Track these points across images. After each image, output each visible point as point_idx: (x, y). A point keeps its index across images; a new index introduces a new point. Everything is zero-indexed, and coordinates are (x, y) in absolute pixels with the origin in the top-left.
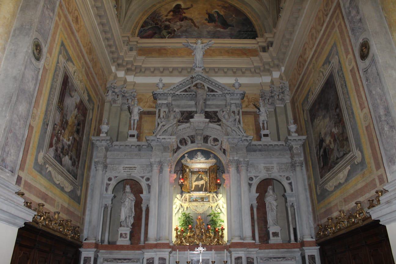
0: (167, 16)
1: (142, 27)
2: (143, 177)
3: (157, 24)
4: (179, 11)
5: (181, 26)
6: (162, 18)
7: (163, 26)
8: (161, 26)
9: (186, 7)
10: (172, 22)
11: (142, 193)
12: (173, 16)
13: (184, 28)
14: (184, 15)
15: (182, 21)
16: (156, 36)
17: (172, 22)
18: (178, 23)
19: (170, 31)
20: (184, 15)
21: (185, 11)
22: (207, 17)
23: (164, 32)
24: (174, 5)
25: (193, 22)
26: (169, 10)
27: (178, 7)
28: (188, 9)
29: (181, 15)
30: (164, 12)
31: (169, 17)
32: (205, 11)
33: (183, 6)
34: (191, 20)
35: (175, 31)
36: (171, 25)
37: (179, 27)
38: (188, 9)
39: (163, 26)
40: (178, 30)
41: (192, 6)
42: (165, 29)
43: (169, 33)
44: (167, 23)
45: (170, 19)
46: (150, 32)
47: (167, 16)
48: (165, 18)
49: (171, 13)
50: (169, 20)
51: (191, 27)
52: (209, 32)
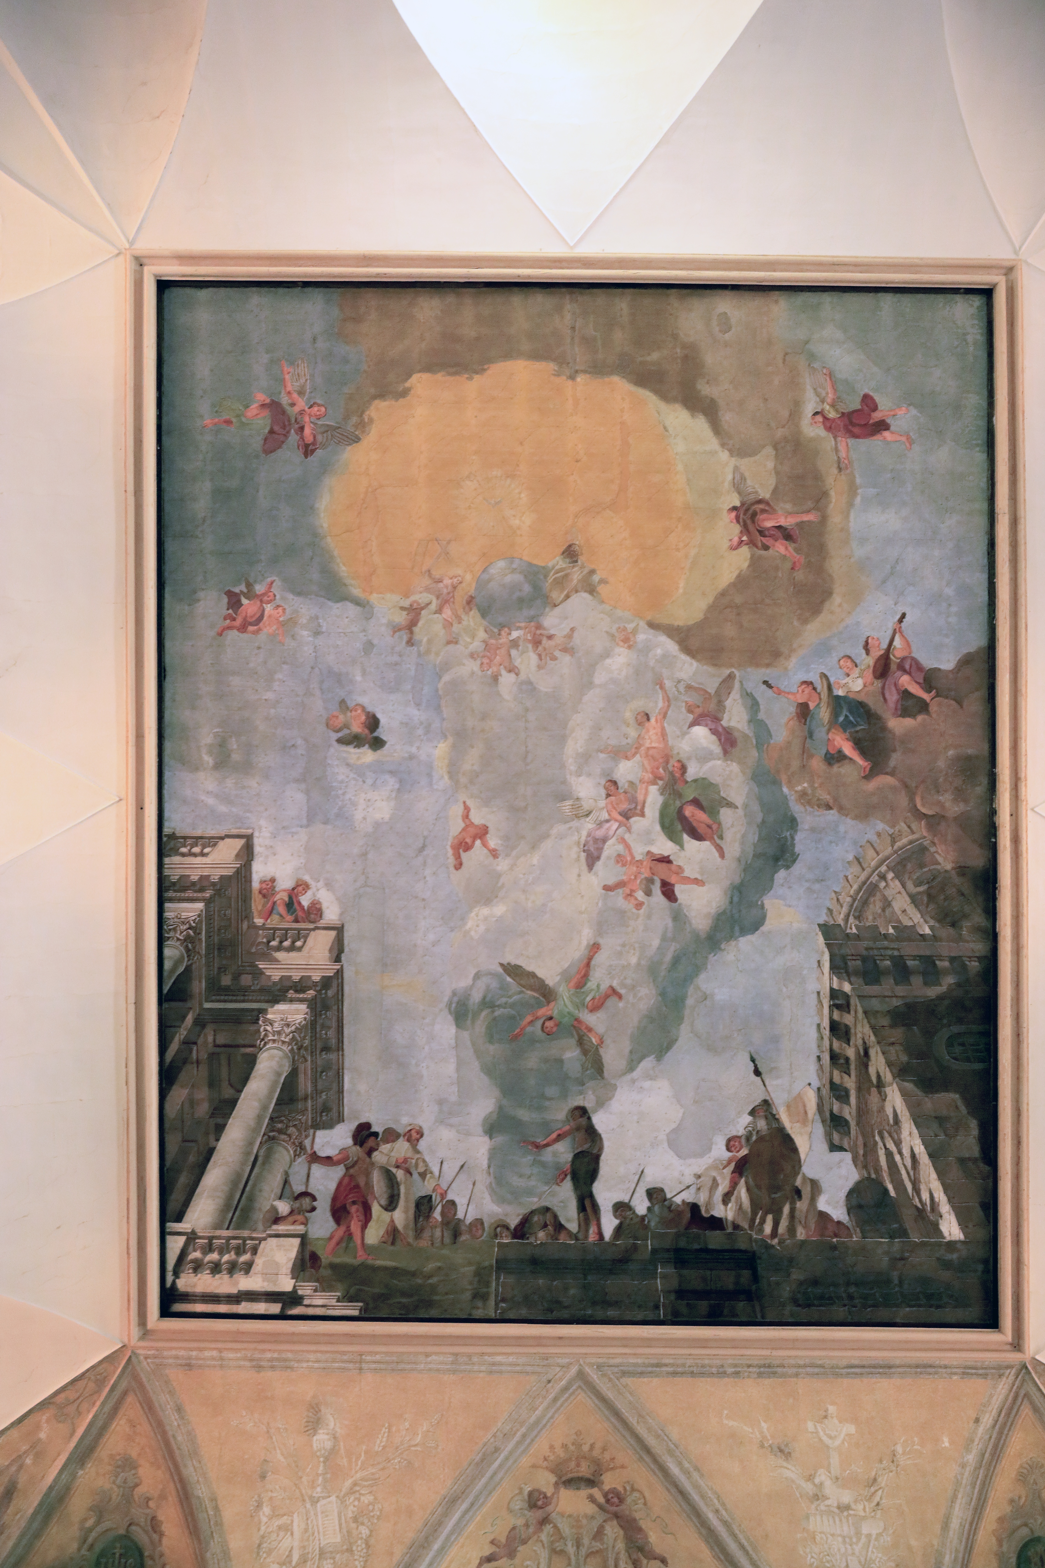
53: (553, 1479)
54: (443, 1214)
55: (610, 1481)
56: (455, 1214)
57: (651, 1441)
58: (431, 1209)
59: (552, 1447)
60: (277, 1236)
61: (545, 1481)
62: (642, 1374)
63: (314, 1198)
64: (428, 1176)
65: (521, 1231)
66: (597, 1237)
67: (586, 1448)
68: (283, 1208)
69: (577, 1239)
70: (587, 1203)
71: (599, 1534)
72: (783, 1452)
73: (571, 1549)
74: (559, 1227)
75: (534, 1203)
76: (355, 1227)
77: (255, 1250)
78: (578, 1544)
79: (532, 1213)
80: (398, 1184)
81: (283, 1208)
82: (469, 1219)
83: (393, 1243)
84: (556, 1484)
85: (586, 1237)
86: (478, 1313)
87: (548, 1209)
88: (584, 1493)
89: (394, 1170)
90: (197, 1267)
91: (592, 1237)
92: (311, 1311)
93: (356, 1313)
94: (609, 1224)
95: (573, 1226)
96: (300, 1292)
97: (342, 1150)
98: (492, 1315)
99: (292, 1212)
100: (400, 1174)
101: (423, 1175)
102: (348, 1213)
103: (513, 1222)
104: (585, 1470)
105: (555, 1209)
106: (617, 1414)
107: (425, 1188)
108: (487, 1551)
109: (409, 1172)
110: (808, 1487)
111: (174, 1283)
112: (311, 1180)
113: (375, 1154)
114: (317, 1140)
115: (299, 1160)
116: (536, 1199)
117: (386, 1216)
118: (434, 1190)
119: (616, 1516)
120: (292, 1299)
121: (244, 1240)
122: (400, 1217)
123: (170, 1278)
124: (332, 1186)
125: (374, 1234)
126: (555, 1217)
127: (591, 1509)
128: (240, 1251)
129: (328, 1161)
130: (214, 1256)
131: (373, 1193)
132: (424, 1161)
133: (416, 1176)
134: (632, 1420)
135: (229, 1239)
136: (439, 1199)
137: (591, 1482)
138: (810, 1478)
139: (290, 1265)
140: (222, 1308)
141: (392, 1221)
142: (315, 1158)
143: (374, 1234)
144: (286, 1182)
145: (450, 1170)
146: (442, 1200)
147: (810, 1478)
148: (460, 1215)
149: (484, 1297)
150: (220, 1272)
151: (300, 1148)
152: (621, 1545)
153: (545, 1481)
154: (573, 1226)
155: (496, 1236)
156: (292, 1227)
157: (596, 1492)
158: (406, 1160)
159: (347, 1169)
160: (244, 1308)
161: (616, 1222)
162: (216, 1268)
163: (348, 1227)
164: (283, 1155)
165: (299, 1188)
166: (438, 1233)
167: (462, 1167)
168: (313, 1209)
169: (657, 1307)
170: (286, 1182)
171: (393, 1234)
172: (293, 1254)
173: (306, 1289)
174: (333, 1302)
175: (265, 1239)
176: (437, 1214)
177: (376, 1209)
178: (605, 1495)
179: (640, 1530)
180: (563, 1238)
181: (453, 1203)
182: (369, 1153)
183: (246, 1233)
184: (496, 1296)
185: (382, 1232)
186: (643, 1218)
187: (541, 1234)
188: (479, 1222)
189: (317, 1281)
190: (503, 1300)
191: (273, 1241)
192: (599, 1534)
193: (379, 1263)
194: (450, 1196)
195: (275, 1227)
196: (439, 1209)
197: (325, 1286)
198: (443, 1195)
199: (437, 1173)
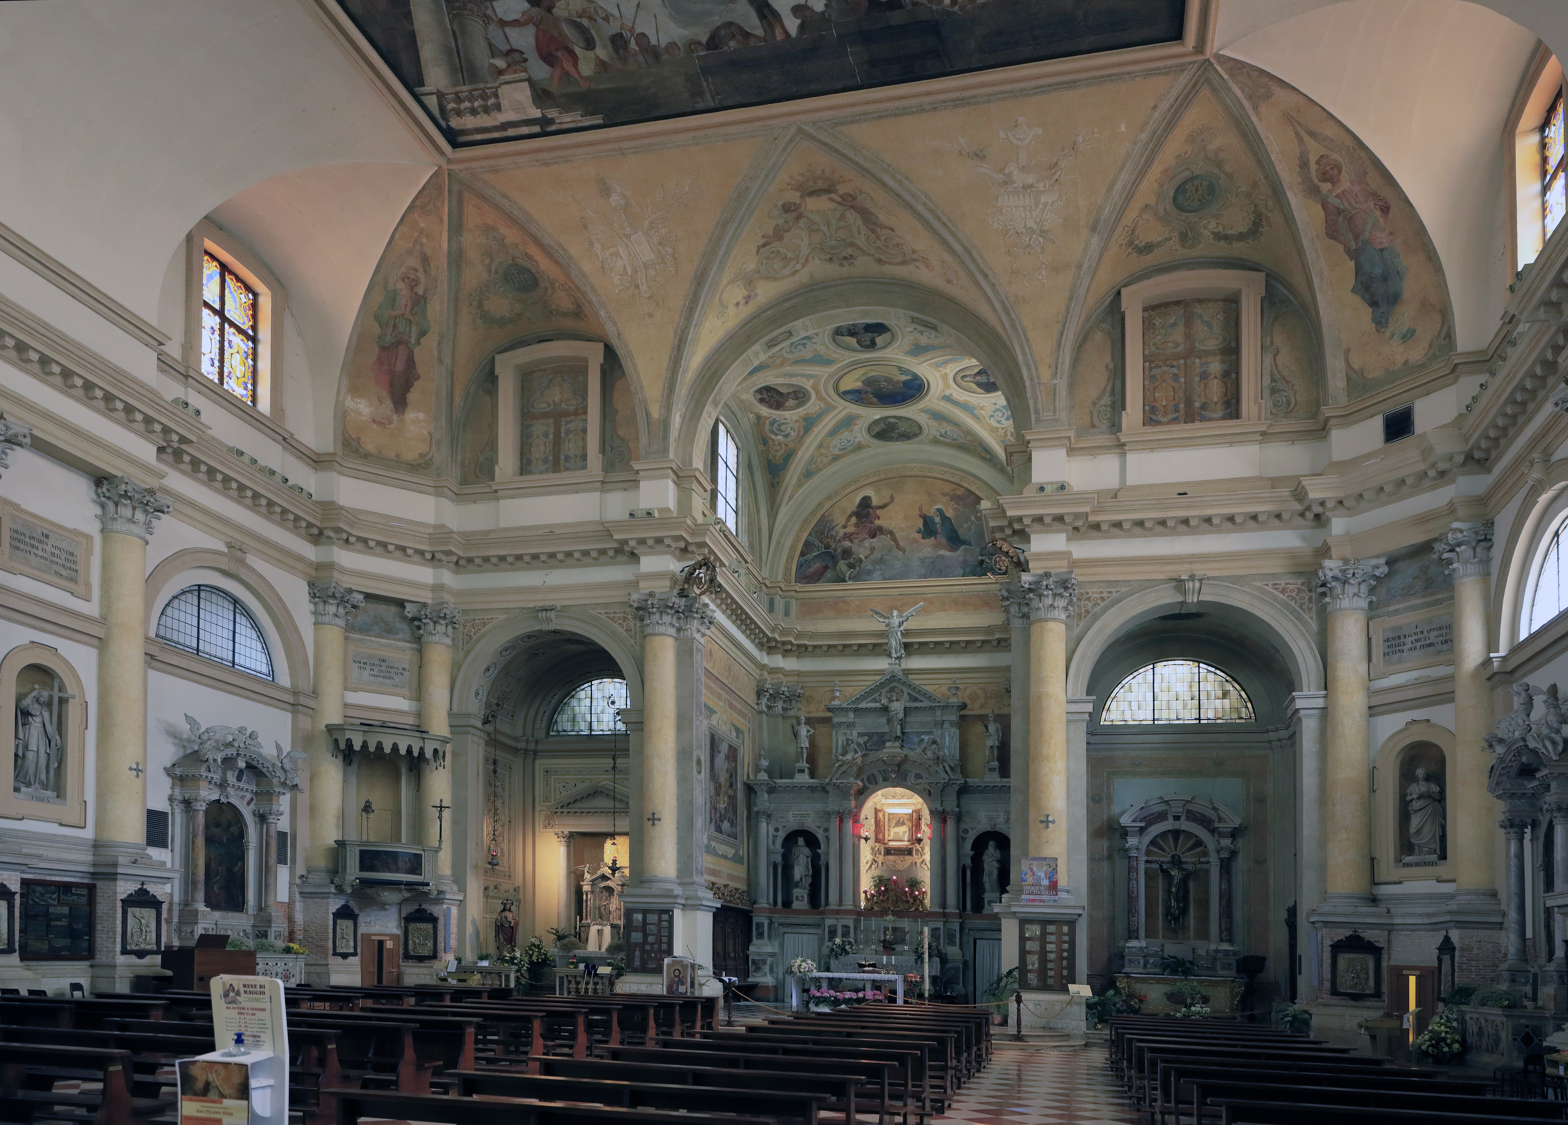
0: (845, 527)
1: (802, 554)
2: (819, 827)
3: (827, 547)
4: (868, 515)
5: (873, 549)
6: (837, 533)
7: (839, 550)
8: (835, 550)
9: (880, 504)
10: (856, 541)
11: (820, 848)
12: (856, 525)
13: (877, 555)
14: (877, 522)
15: (873, 537)
16: (829, 574)
17: (856, 541)
18: (867, 543)
19: (852, 561)
20: (877, 522)
21: (878, 512)
22: (920, 524)
23: (842, 565)
24: (858, 500)
25: (895, 540)
26: (849, 512)
27: (865, 503)
28: (883, 507)
29: (872, 523)
30: (839, 518)
31: (851, 529)
32: (917, 512)
33: (875, 502)
34: (891, 533)
35: (861, 560)
36: (855, 548)
37: (868, 552)
38: (883, 507)
39: (839, 550)
40: (866, 558)
41: (892, 498)
42: (843, 559)
43: (851, 566)
44: (847, 544)
45: (852, 534)
46: (817, 566)
47: (845, 527)
48: (842, 532)
49: (854, 520)
50: (849, 537)
51: (890, 551)
52: (922, 560)
53: (798, 194)
54: (637, 43)
55: (842, 189)
56: (649, 42)
57: (867, 165)
58: (626, 43)
59: (791, 177)
60: (508, 83)
61: (794, 197)
62: (851, 122)
63: (522, 53)
64: (611, 19)
65: (714, 43)
66: (784, 36)
67: (819, 173)
68: (501, 63)
69: (766, 41)
70: (766, 12)
71: (842, 217)
72: (979, 156)
73: (824, 228)
74: (747, 35)
75: (717, 21)
76: (568, 66)
77: (496, 96)
78: (828, 224)
79: (719, 28)
80: (588, 30)
81: (501, 63)
82: (663, 44)
83: (606, 72)
84: (801, 196)
85: (774, 37)
86: (700, 106)
87: (730, 24)
88: (824, 197)
89: (579, 20)
90: (459, 113)
91: (779, 36)
92: (565, 126)
93: (601, 122)
94: (792, 25)
95: (760, 32)
96: (549, 116)
97: (524, 13)
98: (712, 104)
99: (509, 65)
100: (585, 22)
101: (606, 19)
102: (557, 57)
103: (704, 39)
104: (821, 184)
105: (738, 22)
106: (836, 151)
107: (613, 28)
108: (762, 242)
109: (591, 18)
110: (1000, 177)
111: (448, 125)
112: (511, 39)
113: (554, 10)
114: (497, 9)
115: (491, 27)
116: (717, 18)
117: (590, 54)
118: (622, 28)
119: (852, 207)
120: (544, 121)
121: (483, 90)
122: (602, 52)
123: (443, 123)
124: (532, 41)
125: (586, 68)
126: (740, 28)
127: (832, 205)
128: (484, 97)
129: (515, 23)
130: (467, 104)
131: (569, 40)
132: (601, 7)
133: (599, 20)
134: (851, 155)
135: (470, 92)
136: (629, 35)
137: (828, 191)
138: (1001, 170)
139: (530, 100)
140: (496, 135)
141: (597, 57)
142: (503, 23)
143: (586, 68)
144: (491, 45)
145: (628, 10)
146: (632, 35)
147: (1001, 170)
148: (653, 41)
149: (701, 94)
150: (478, 113)
151: (487, 20)
152: (859, 222)
153: (794, 197)
154: (760, 32)
155: (692, 51)
156: (516, 76)
157: (833, 196)
158: (584, 10)
159: (537, 26)
160: (511, 132)
161: (798, 21)
162: (474, 112)
163: (562, 67)
164: (475, 27)
165: (505, 47)
166: (641, 58)
167: (638, 5)
168: (526, 60)
169: (855, 76)
170: (491, 45)
171: (602, 65)
172: (528, 92)
173: (552, 113)
174: (579, 118)
175: (499, 87)
176: (633, 45)
177: (578, 51)
178: (841, 197)
179: (872, 214)
180: (752, 42)
181: (643, 35)
182: (549, 10)
183: (481, 86)
184: (711, 91)
185: (592, 66)
186: (823, 13)
187: (732, 43)
188: (673, 45)
189: (558, 107)
190: (718, 94)
191: (506, 88)
192: (842, 217)
193: (601, 87)
194: (638, 30)
195: (502, 77)
196: (633, 41)
197: (566, 109)
198: (632, 30)
199: (618, 15)
